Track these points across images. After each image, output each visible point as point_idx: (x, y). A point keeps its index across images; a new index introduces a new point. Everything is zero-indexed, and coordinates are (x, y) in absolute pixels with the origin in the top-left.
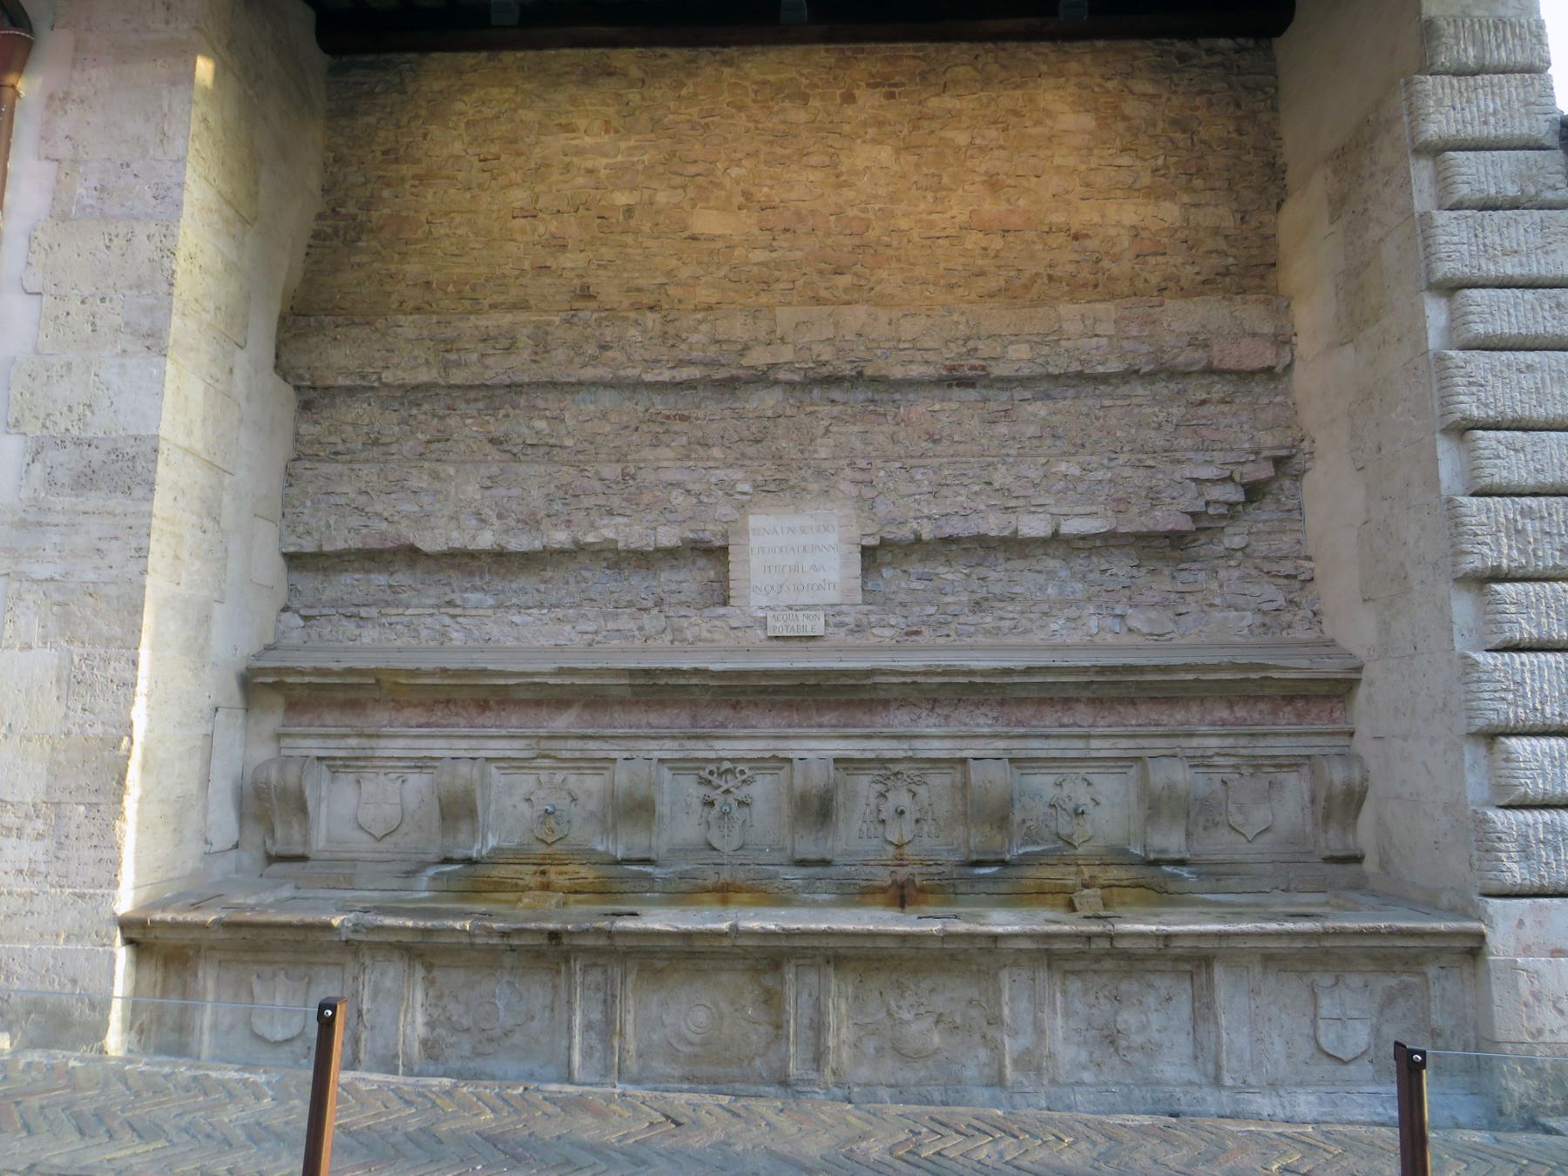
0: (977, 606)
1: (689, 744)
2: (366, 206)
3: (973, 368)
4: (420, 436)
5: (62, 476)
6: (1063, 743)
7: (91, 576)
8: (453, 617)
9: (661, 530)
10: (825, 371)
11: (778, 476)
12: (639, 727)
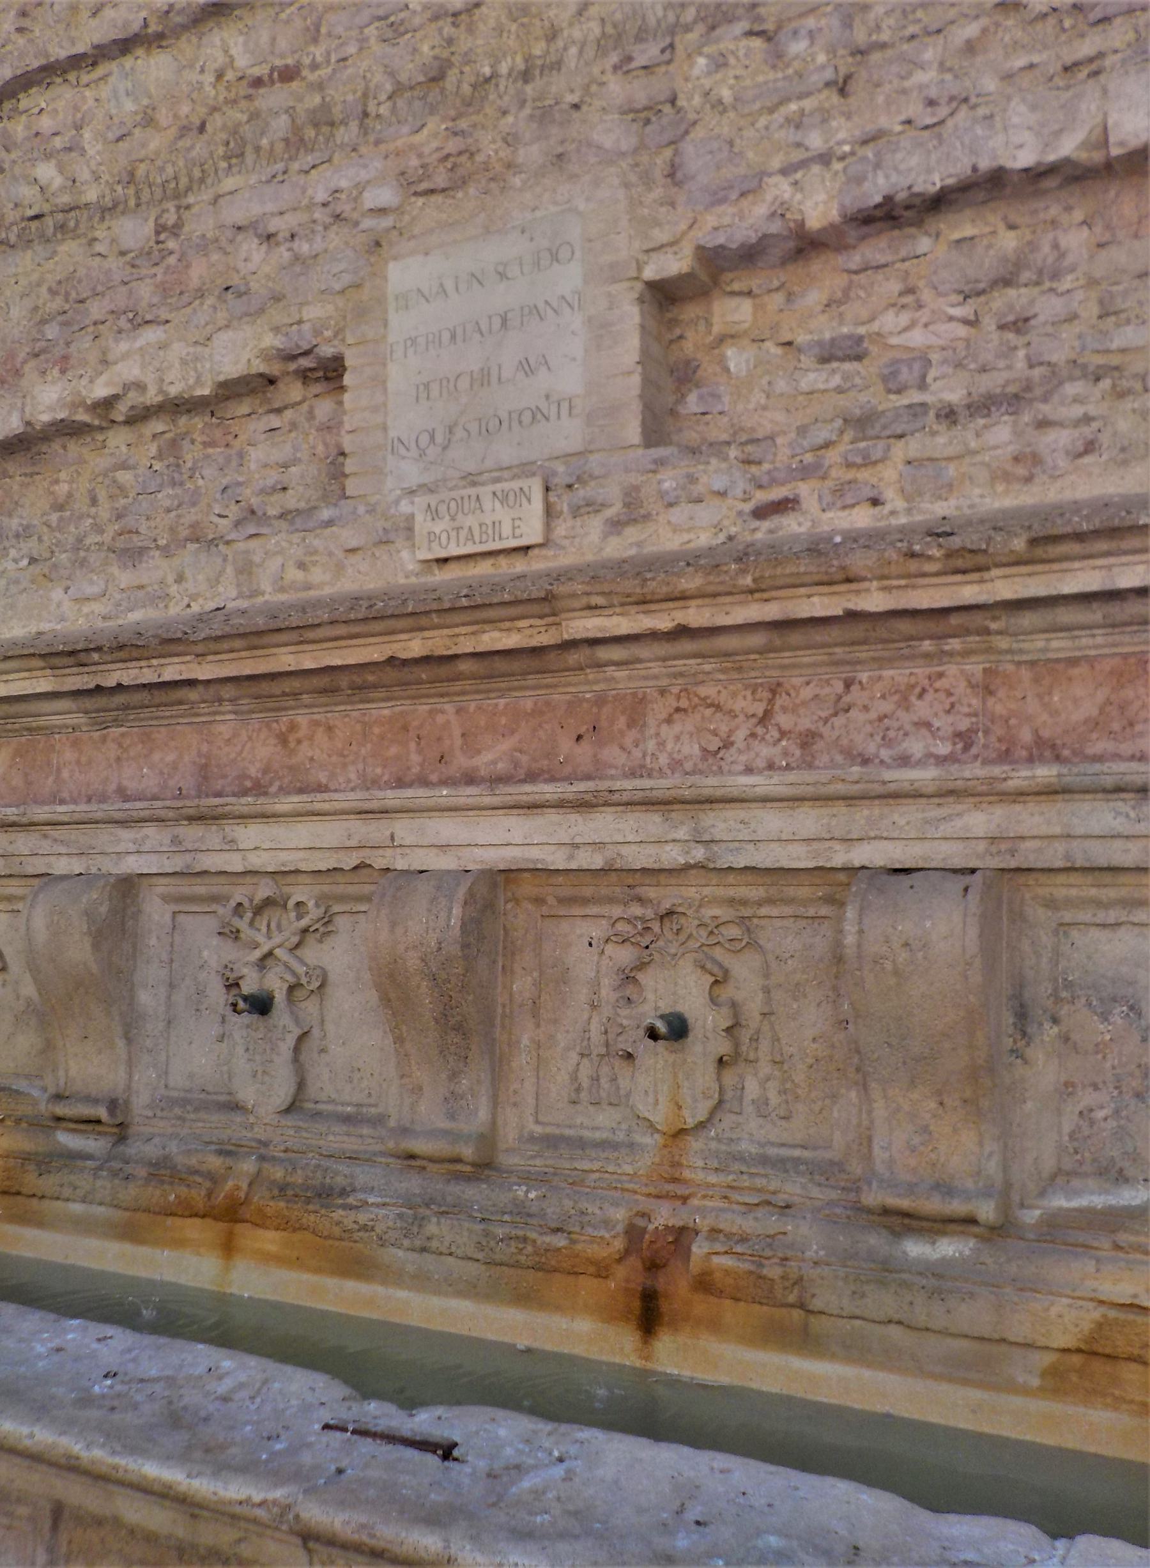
1: (191, 833)
12: (103, 798)
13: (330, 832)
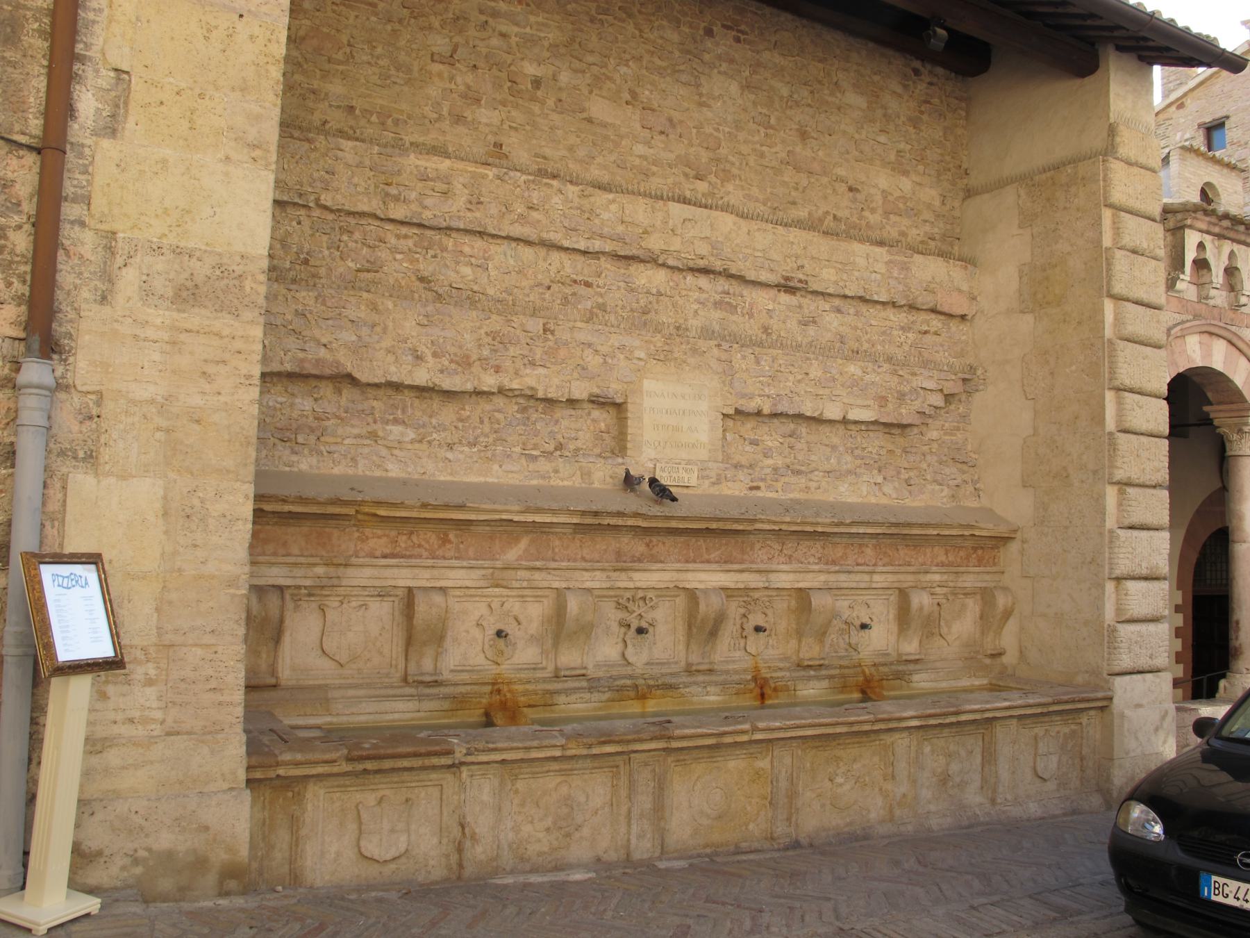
3: (800, 281)
4: (351, 264)
6: (858, 577)
7: (197, 400)
8: (389, 448)
9: (575, 384)
10: (702, 263)
11: (666, 348)
12: (575, 560)
13: (667, 576)
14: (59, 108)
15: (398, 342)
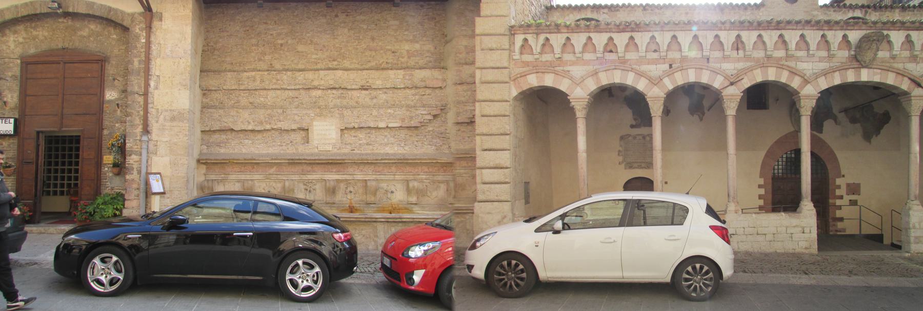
0: (368, 144)
2: (216, 43)
5: (167, 118)
14: (147, 85)
15: (243, 119)
